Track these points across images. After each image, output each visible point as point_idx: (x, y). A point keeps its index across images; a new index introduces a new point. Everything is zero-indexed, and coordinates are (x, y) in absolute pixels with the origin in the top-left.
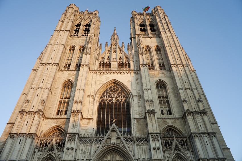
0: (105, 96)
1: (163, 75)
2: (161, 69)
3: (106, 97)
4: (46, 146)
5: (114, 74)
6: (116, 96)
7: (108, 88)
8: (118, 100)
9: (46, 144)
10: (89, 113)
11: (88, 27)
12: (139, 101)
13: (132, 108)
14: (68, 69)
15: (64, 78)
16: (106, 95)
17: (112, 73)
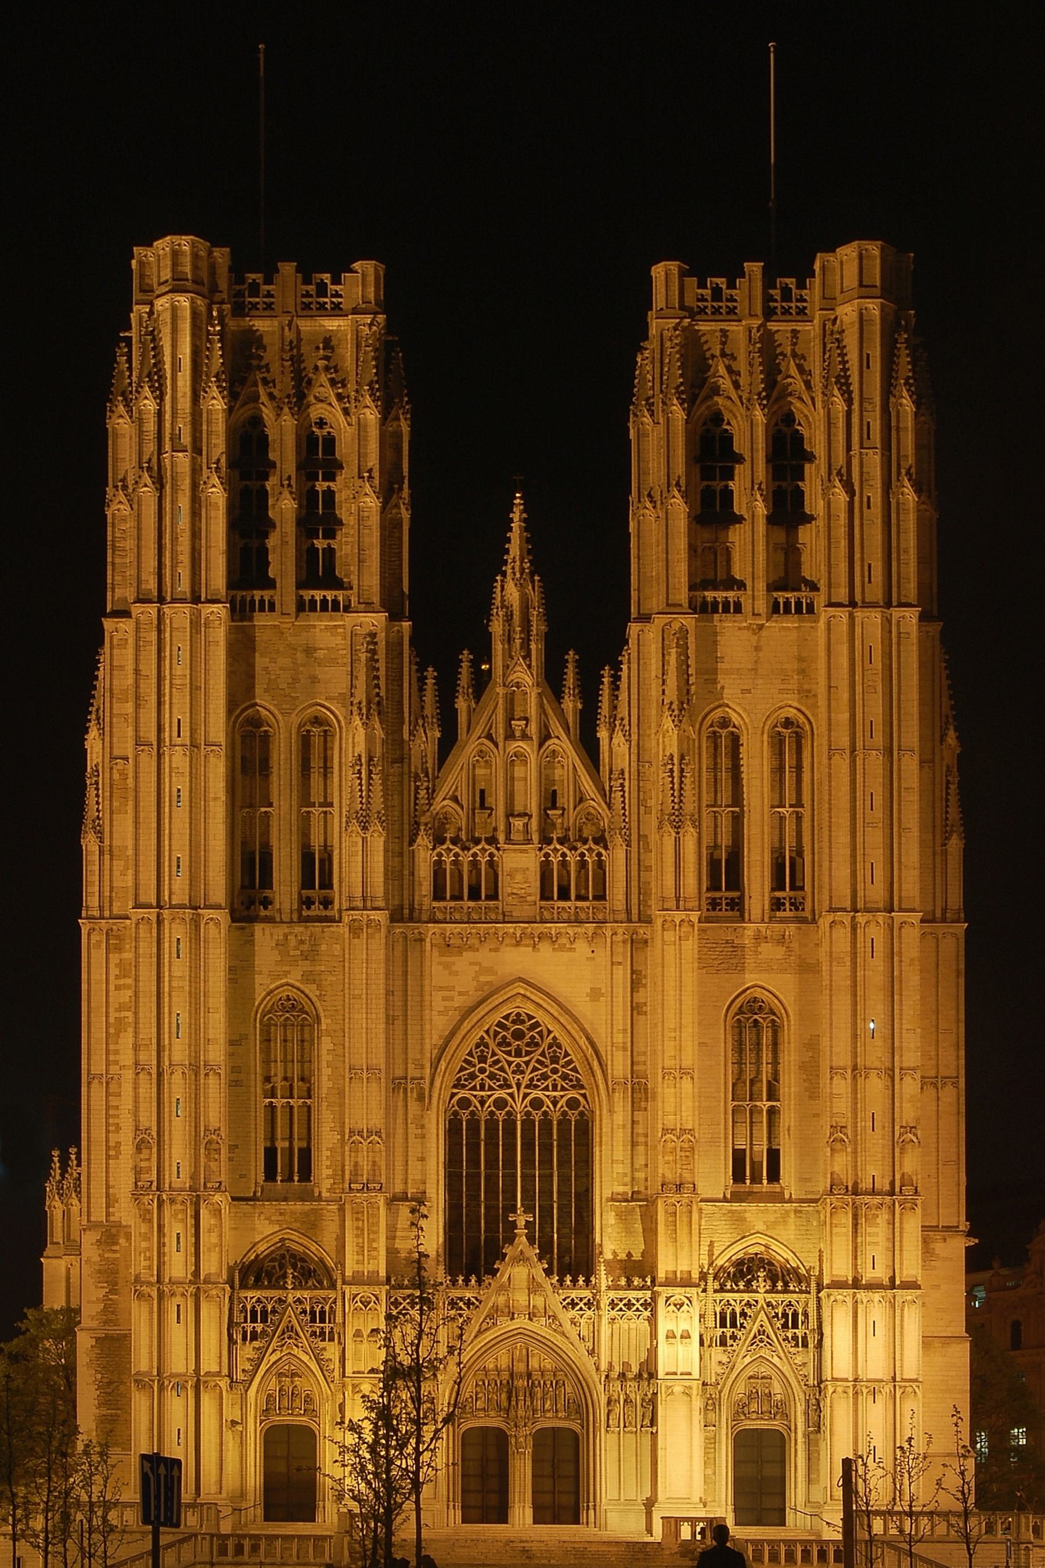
0: (472, 1076)
1: (780, 952)
2: (777, 905)
3: (477, 1082)
4: (264, 1320)
5: (518, 944)
6: (527, 1077)
7: (487, 1032)
8: (537, 1104)
9: (265, 1313)
10: (410, 1177)
11: (321, 486)
12: (639, 1116)
13: (601, 1151)
14: (266, 903)
15: (260, 973)
16: (482, 1071)
17: (507, 941)
